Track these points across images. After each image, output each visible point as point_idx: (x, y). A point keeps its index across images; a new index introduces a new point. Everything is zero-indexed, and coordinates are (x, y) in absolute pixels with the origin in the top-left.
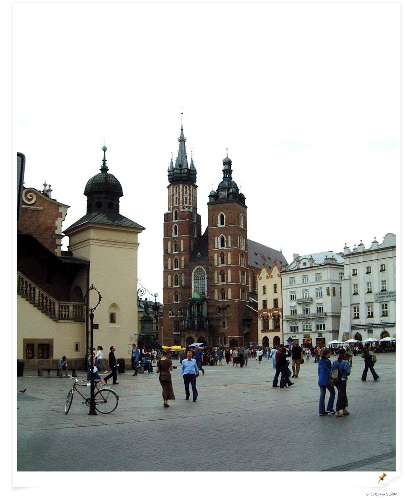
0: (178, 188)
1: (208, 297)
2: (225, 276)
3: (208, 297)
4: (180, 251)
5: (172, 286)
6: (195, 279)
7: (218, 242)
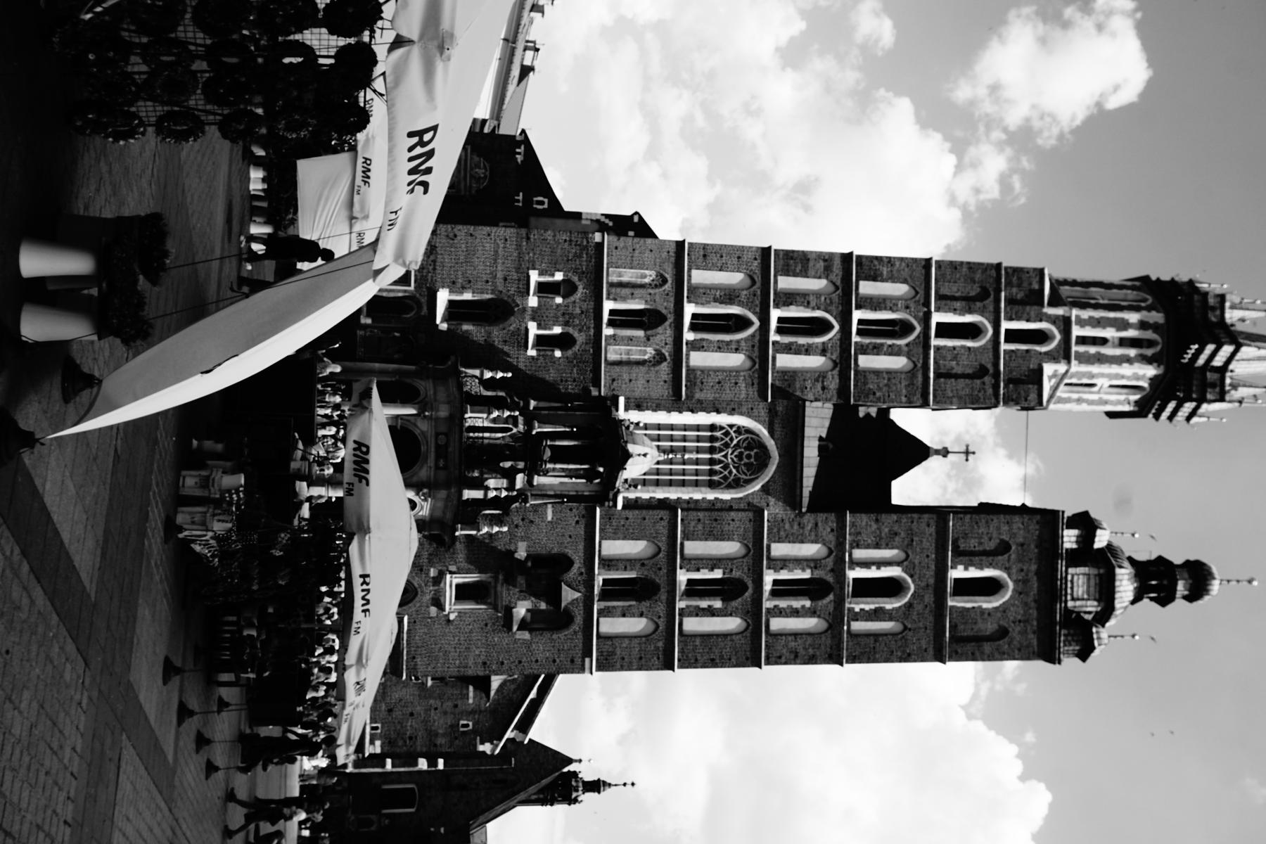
0: (1149, 352)
1: (620, 506)
2: (718, 604)
3: (620, 506)
4: (863, 350)
5: (699, 294)
6: (713, 427)
7: (878, 568)
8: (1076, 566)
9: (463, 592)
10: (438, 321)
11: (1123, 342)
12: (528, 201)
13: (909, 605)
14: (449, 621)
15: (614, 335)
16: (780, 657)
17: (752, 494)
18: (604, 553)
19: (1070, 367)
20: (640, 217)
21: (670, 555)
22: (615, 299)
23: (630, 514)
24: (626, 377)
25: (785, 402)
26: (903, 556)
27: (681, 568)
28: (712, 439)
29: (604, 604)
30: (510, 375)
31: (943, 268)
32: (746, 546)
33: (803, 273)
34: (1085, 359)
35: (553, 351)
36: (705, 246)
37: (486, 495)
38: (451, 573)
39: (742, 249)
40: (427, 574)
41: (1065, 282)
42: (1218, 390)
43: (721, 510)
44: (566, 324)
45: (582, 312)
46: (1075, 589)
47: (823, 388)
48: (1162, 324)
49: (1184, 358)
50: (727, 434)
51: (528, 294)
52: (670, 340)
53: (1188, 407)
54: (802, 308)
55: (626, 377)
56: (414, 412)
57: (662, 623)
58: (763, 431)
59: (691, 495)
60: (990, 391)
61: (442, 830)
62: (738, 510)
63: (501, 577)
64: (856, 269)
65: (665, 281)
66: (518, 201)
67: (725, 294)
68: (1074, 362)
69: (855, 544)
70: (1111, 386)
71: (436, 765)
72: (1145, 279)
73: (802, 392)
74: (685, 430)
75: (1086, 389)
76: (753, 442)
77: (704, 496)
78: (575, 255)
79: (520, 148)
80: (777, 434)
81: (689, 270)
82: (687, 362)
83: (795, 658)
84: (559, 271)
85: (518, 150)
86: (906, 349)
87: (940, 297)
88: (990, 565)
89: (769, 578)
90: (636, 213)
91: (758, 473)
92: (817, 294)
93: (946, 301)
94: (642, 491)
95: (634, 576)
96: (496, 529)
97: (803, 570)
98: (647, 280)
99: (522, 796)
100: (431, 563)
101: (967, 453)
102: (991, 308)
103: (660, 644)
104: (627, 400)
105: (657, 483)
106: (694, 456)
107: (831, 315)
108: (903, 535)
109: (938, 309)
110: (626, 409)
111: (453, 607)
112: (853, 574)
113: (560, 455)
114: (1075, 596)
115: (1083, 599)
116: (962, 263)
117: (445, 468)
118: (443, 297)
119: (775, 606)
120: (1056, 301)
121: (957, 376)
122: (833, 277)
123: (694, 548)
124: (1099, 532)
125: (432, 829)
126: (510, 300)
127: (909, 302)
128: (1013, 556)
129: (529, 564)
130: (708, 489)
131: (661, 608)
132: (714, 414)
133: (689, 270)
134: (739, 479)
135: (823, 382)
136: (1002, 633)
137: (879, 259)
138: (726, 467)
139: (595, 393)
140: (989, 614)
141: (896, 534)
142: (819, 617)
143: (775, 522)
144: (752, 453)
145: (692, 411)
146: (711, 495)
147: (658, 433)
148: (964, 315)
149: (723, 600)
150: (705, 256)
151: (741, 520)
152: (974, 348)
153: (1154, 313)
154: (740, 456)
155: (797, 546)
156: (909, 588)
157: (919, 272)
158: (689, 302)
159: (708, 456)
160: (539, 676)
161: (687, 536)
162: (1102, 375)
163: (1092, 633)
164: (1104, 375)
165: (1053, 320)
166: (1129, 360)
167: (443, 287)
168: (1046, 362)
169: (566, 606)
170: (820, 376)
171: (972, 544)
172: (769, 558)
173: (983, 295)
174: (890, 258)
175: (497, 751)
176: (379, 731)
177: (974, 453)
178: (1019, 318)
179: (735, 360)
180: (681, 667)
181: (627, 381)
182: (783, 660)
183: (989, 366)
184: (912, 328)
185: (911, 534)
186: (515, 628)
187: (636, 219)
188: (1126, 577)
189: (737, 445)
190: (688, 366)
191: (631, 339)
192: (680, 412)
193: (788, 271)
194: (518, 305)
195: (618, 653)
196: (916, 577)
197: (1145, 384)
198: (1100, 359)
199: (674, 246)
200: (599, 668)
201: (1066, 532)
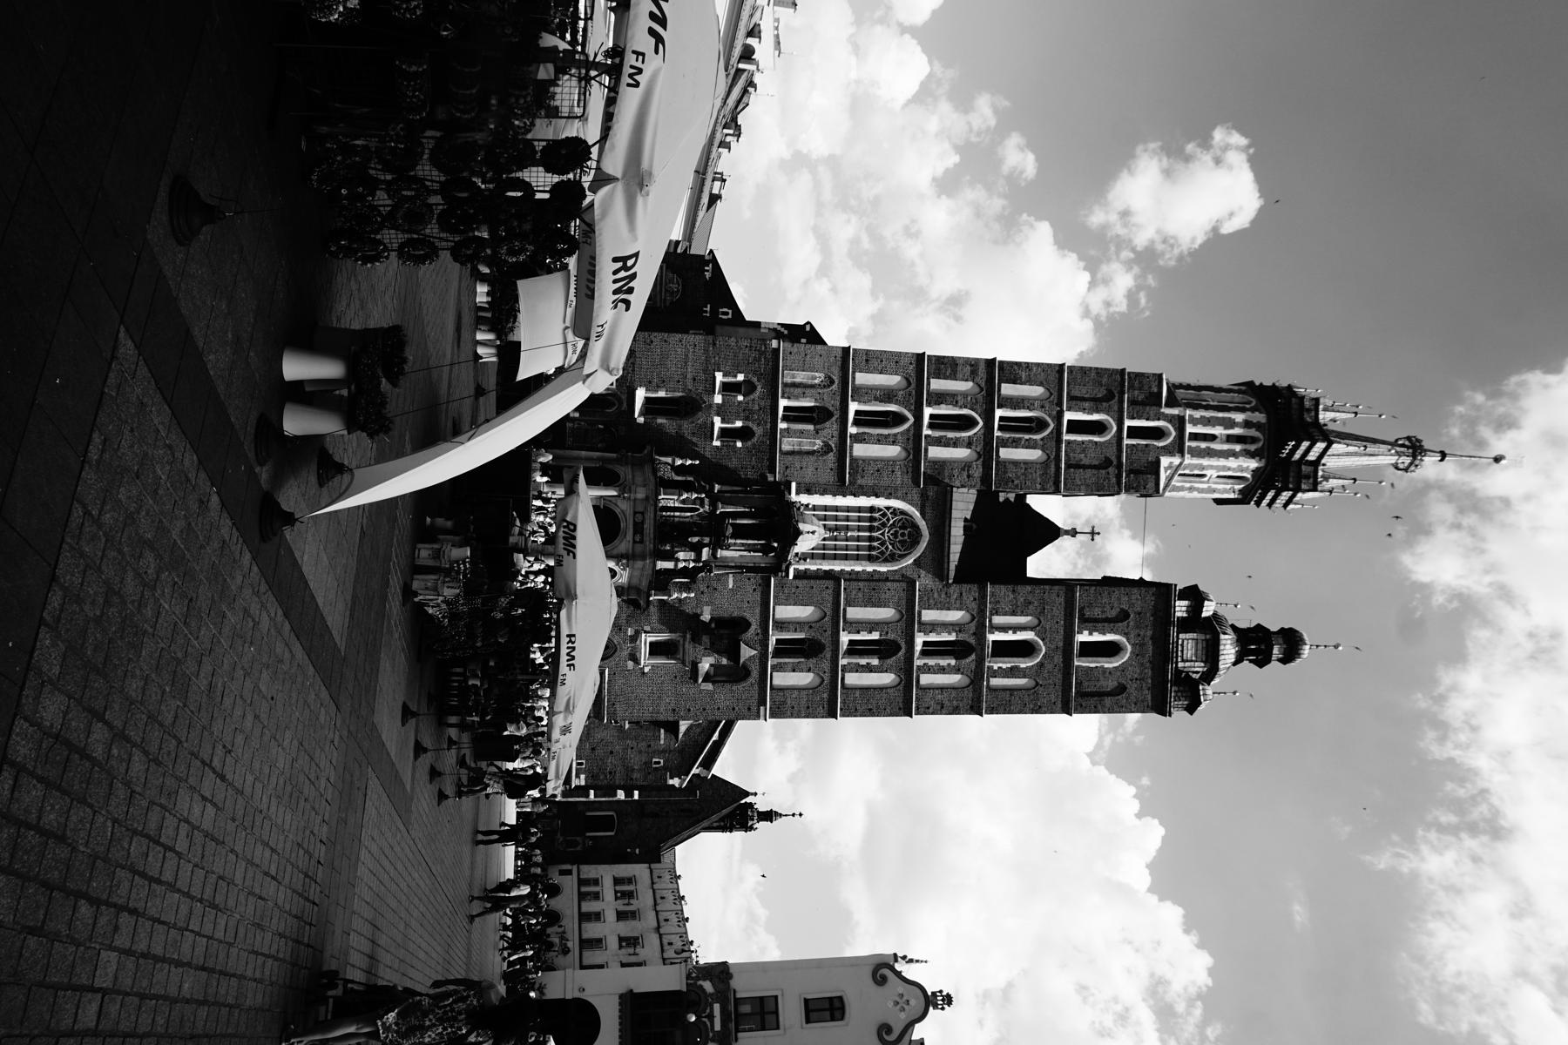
0: (1252, 448)
1: (791, 577)
2: (875, 662)
3: (791, 577)
4: (1004, 443)
5: (862, 393)
6: (872, 509)
7: (1014, 632)
8: (1186, 632)
9: (656, 649)
10: (636, 415)
11: (1230, 439)
12: (714, 312)
13: (1041, 665)
14: (644, 673)
15: (788, 428)
16: (928, 708)
17: (906, 567)
18: (777, 616)
19: (1184, 460)
20: (811, 325)
21: (834, 619)
22: (789, 398)
23: (799, 583)
24: (798, 465)
25: (936, 488)
26: (1036, 622)
27: (843, 630)
28: (872, 519)
29: (776, 661)
30: (697, 462)
31: (1074, 373)
32: (900, 612)
33: (953, 377)
34: (1197, 453)
35: (735, 442)
36: (867, 352)
37: (676, 565)
38: (645, 632)
39: (900, 354)
40: (626, 632)
41: (1181, 386)
42: (1311, 481)
43: (879, 580)
44: (746, 419)
45: (761, 409)
46: (1185, 652)
47: (969, 476)
48: (1264, 424)
49: (1283, 453)
50: (884, 515)
51: (714, 393)
52: (836, 434)
53: (1286, 495)
54: (951, 406)
55: (798, 465)
56: (615, 493)
57: (827, 677)
58: (917, 514)
59: (852, 568)
60: (1114, 480)
61: (637, 851)
62: (893, 581)
63: (688, 636)
64: (999, 373)
65: (832, 382)
66: (706, 312)
67: (884, 394)
68: (1187, 456)
69: (994, 612)
70: (1218, 477)
71: (632, 796)
72: (1250, 384)
73: (950, 479)
74: (848, 512)
75: (1197, 479)
76: (907, 522)
77: (864, 568)
78: (755, 359)
79: (708, 266)
80: (928, 515)
81: (854, 373)
83: (941, 709)
84: (740, 373)
85: (706, 268)
86: (1041, 443)
87: (1071, 398)
88: (1112, 631)
89: (919, 640)
90: (808, 323)
91: (911, 548)
92: (965, 394)
93: (1076, 402)
94: (810, 564)
95: (801, 636)
96: (685, 595)
97: (950, 633)
98: (816, 381)
99: (705, 823)
100: (629, 624)
101: (1093, 533)
102: (1116, 408)
103: (825, 695)
104: (798, 485)
105: (824, 557)
106: (855, 534)
107: (977, 413)
108: (1036, 604)
109: (1069, 409)
110: (798, 493)
111: (647, 662)
112: (992, 637)
113: (740, 532)
114: (1185, 658)
115: (1192, 661)
116: (1091, 368)
117: (641, 542)
118: (641, 394)
119: (924, 664)
120: (1172, 402)
121: (1084, 467)
122: (978, 379)
123: (854, 613)
124: (1206, 603)
125: (629, 850)
126: (698, 397)
128: (1131, 623)
129: (713, 625)
130: (868, 563)
131: (826, 665)
132: (874, 498)
133: (854, 373)
134: (894, 554)
135: (968, 471)
136: (1121, 689)
137: (1018, 364)
138: (883, 544)
139: (771, 478)
140: (1110, 673)
141: (1030, 603)
142: (962, 674)
143: (924, 591)
144: (906, 532)
145: (855, 496)
146: (870, 569)
147: (824, 514)
148: (1092, 414)
149: (879, 658)
150: (867, 360)
151: (895, 590)
152: (1100, 442)
153: (1257, 413)
154: (895, 535)
155: (944, 612)
156: (1041, 650)
157: (1053, 376)
158: (853, 400)
159: (868, 534)
160: (721, 722)
161: (849, 603)
162: (1211, 467)
163: (1199, 690)
164: (1213, 467)
165: (1170, 419)
166: (1234, 454)
167: (641, 386)
168: (1163, 456)
169: (744, 662)
170: (966, 466)
171: (1096, 612)
172: (919, 622)
173: (1109, 397)
174: (1028, 363)
175: (684, 785)
176: (584, 766)
177: (1099, 534)
178: (1140, 418)
179: (893, 451)
180: (843, 715)
182: (931, 710)
183: (1114, 459)
185: (1043, 603)
186: (700, 680)
187: (808, 328)
188: (1229, 642)
189: (893, 524)
190: (851, 456)
191: (802, 432)
192: (844, 496)
194: (705, 402)
195: (789, 703)
196: (1047, 640)
197: (1249, 476)
198: (1210, 453)
199: (840, 352)
200: (772, 716)
201: (1178, 603)
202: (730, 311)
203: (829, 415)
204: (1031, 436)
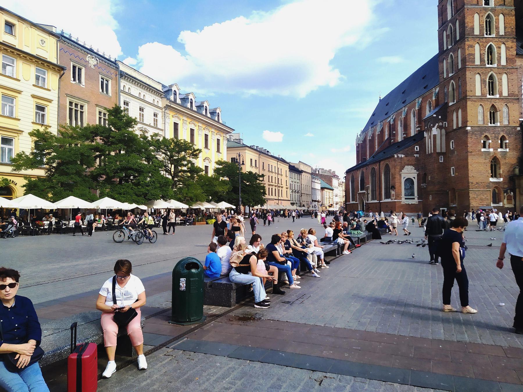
4: (498, 32)
12: (417, 153)
35: (506, 143)
47: (512, 48)
82: (506, 97)
92: (480, 50)
127: (480, 16)
135: (510, 48)
181: (514, 118)
184: (489, 15)
191: (500, 117)
193: (473, 61)
202: (416, 147)
203: (493, 106)
204: (494, 21)
